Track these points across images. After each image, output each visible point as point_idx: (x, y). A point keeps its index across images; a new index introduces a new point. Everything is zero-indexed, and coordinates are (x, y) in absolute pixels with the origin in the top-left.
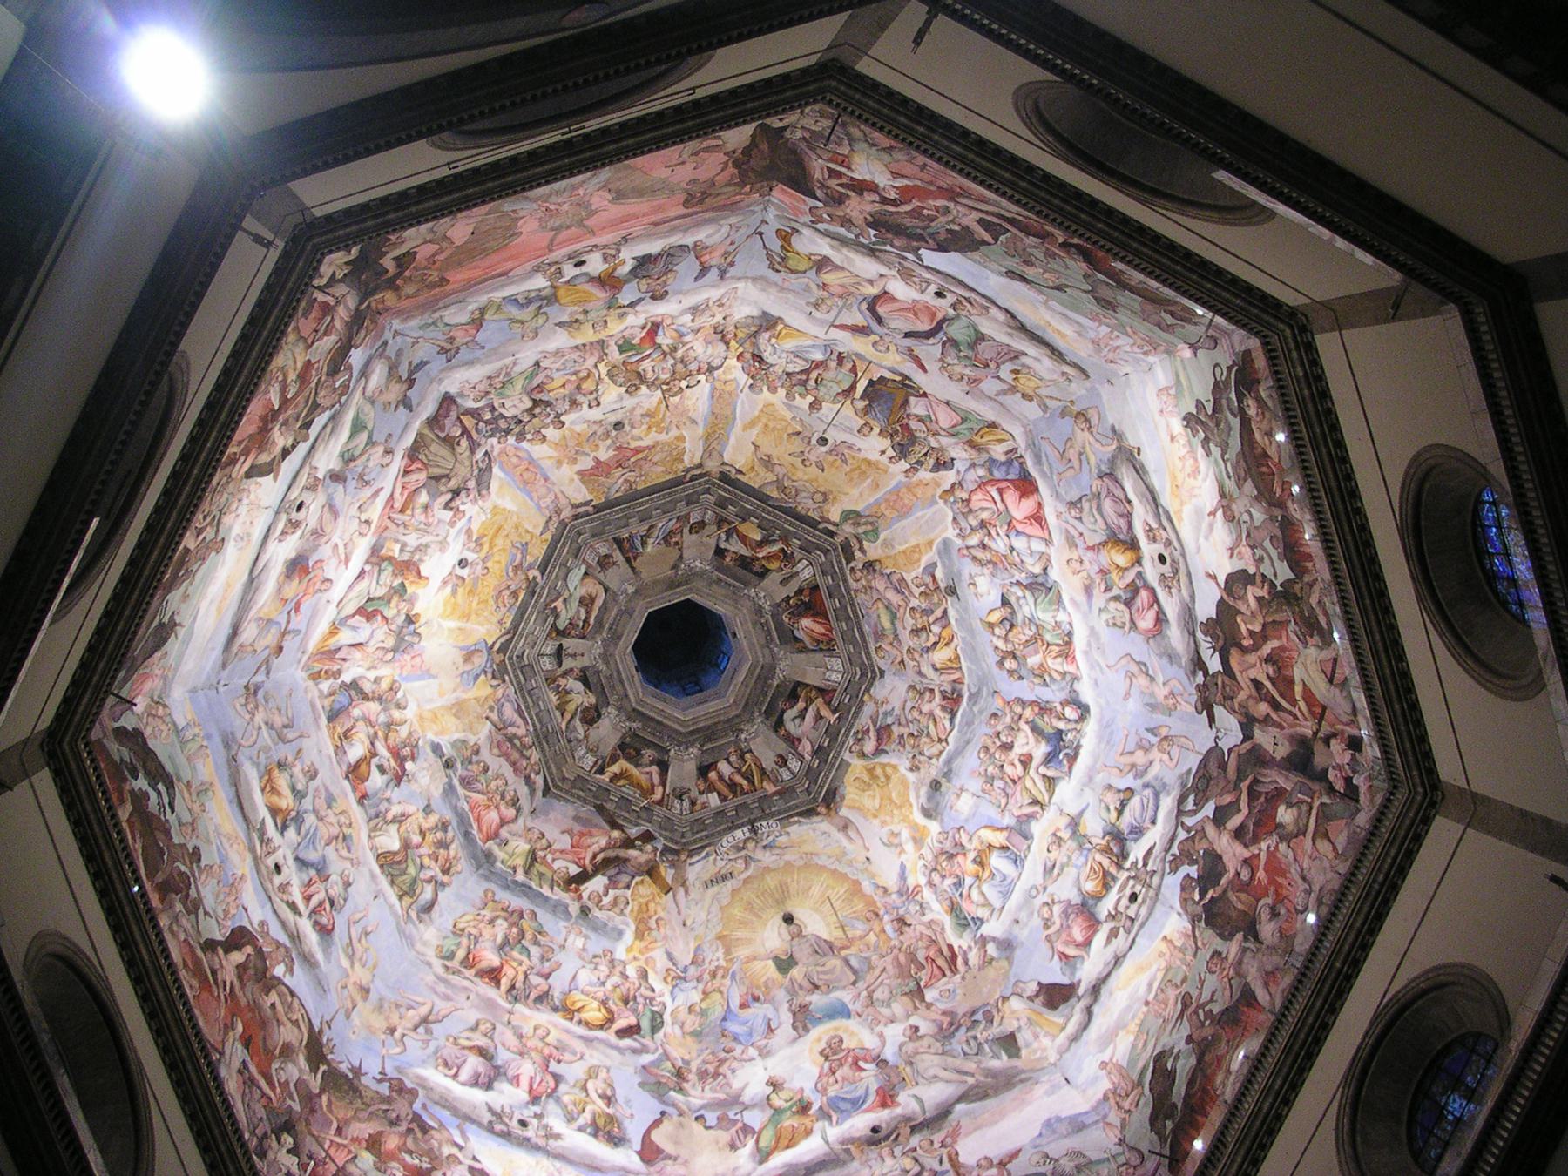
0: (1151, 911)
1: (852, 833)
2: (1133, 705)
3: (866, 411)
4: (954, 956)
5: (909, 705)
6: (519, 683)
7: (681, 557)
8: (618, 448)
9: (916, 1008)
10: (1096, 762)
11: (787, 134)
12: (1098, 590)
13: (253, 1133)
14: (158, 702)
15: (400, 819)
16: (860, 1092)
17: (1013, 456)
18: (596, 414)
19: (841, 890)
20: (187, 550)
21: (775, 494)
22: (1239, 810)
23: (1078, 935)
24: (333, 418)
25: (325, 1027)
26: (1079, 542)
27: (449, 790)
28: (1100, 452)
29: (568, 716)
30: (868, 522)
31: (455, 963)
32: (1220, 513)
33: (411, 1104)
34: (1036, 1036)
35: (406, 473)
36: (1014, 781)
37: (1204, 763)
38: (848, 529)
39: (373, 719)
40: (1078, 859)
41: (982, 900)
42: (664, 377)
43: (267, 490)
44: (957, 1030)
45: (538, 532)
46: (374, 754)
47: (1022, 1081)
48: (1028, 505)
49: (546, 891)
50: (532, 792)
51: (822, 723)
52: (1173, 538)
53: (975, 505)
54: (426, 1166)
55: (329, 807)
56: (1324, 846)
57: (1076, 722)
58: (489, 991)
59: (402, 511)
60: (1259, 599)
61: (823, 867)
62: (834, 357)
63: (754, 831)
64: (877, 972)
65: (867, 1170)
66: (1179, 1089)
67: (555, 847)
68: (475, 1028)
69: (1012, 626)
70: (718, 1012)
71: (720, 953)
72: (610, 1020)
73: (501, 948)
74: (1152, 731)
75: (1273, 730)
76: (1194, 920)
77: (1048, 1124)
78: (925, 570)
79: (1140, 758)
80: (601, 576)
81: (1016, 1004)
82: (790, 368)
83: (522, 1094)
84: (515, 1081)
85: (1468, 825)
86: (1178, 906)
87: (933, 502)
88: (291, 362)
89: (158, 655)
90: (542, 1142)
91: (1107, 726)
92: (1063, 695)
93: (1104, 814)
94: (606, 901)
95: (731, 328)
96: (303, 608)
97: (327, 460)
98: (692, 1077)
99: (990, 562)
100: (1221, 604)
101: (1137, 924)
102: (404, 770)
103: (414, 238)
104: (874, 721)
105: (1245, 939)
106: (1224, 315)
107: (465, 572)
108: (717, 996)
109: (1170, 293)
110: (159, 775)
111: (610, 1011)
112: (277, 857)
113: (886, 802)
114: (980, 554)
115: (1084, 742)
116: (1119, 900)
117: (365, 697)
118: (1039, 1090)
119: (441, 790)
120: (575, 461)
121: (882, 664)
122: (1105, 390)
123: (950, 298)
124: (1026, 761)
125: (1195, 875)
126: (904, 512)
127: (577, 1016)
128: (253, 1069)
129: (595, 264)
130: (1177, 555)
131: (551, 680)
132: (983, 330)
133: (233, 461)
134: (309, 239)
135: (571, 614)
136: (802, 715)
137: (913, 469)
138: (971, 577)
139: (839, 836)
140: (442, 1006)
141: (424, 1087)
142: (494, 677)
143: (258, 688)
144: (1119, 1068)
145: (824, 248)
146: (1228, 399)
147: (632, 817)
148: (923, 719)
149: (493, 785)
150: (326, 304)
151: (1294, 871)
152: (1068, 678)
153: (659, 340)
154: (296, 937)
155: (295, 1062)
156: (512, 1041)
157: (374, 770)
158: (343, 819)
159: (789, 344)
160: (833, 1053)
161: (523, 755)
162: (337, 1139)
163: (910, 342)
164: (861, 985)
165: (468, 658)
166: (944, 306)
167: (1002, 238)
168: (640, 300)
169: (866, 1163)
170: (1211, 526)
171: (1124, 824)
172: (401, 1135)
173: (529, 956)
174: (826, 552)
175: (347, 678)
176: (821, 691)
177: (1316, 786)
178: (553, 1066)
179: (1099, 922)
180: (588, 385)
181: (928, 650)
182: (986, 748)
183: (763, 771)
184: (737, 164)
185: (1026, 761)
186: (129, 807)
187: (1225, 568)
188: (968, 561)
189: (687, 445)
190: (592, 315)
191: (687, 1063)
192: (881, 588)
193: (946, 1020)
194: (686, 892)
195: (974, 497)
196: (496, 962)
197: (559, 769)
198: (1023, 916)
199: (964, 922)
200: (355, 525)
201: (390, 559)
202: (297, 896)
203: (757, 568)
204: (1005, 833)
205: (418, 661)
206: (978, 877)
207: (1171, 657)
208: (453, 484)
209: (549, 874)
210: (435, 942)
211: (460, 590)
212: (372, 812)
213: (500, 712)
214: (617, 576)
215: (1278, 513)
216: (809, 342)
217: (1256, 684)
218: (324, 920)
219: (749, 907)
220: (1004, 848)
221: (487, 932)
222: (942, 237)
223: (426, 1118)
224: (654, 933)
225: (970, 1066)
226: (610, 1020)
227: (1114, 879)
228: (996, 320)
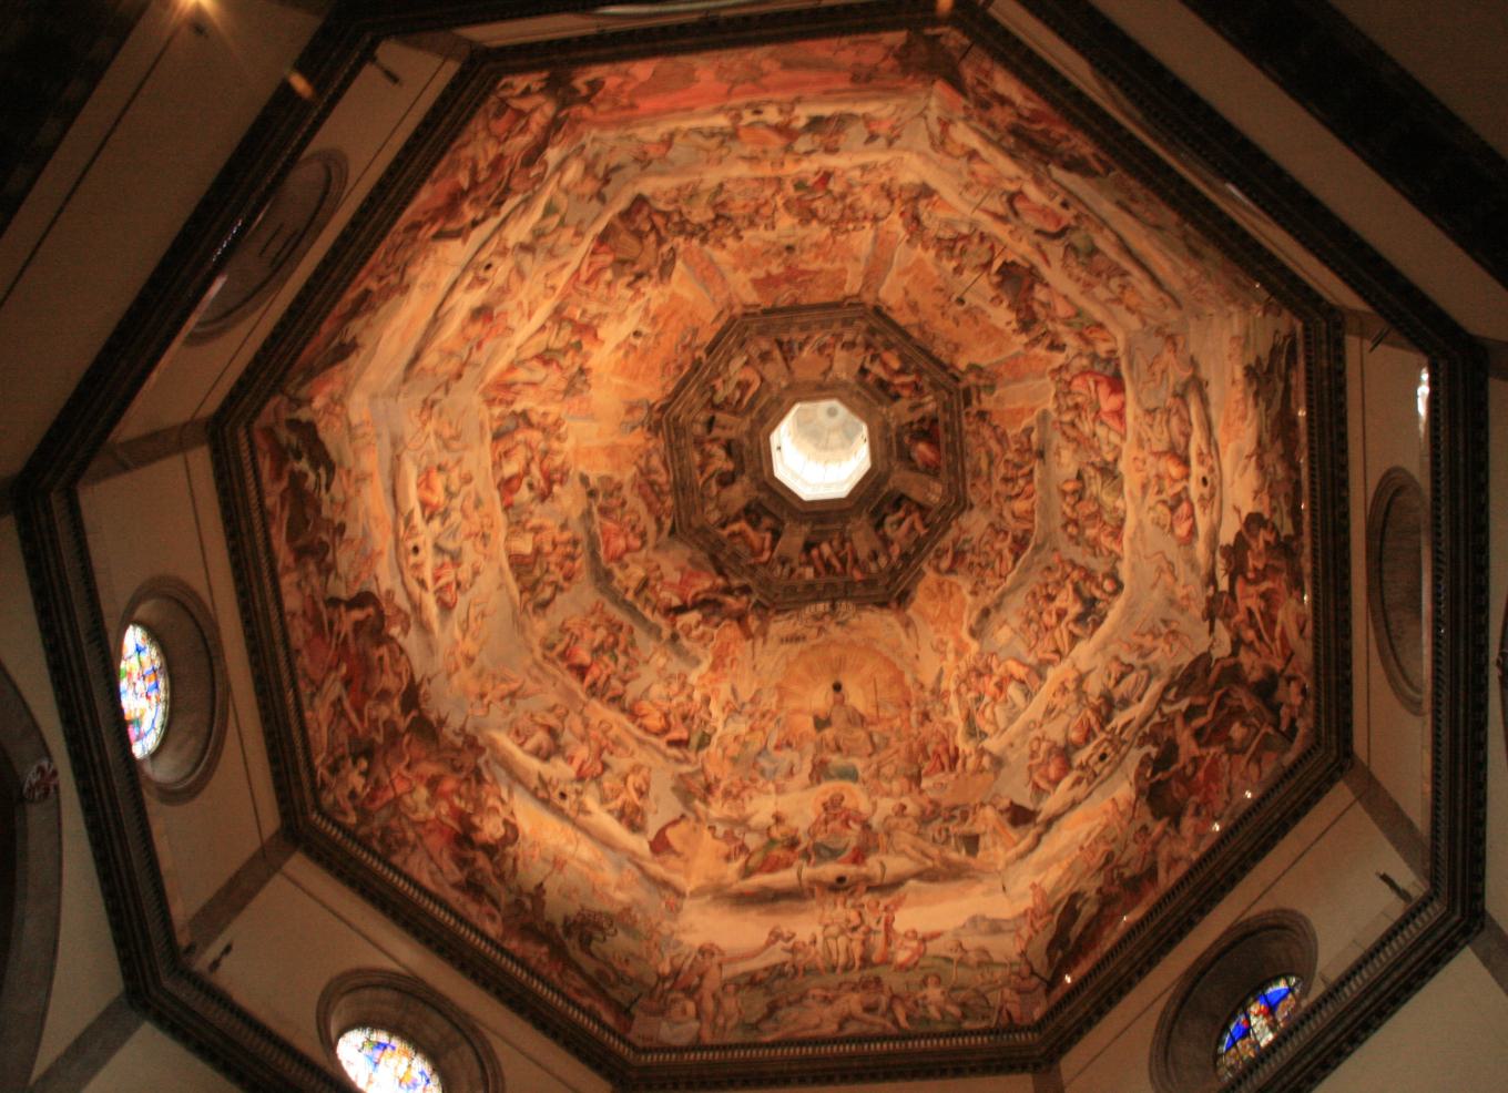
0: (1111, 773)
1: (911, 631)
2: (1156, 594)
3: (999, 285)
5: (985, 539)
6: (670, 440)
7: (830, 368)
8: (789, 267)
9: (910, 790)
11: (943, 40)
12: (1153, 490)
13: (330, 753)
14: (338, 401)
15: (537, 530)
16: (841, 845)
17: (1111, 358)
18: (771, 235)
19: (887, 675)
20: (367, 292)
21: (916, 334)
22: (1206, 713)
23: (1053, 771)
25: (425, 682)
26: (1147, 445)
27: (587, 515)
28: (1178, 374)
29: (706, 475)
30: (988, 379)
31: (554, 654)
32: (1254, 458)
33: (476, 759)
34: (995, 844)
35: (594, 253)
36: (1047, 629)
37: (1194, 664)
38: (971, 379)
39: (534, 445)
40: (1073, 710)
43: (456, 253)
44: (936, 818)
45: (711, 320)
47: (970, 877)
49: (647, 613)
50: (660, 529)
56: (1253, 769)
58: (575, 684)
59: (588, 282)
60: (1267, 543)
61: (878, 653)
62: (977, 233)
63: (833, 607)
65: (818, 911)
66: (1077, 929)
67: (667, 579)
68: (552, 709)
69: (1080, 499)
70: (756, 746)
71: (774, 700)
72: (666, 730)
74: (1165, 622)
75: (1254, 656)
76: (1140, 792)
77: (974, 920)
78: (1024, 431)
79: (1148, 641)
80: (760, 368)
81: (989, 812)
82: (941, 234)
83: (571, 771)
84: (570, 760)
85: (1359, 798)
86: (1132, 776)
87: (1042, 376)
89: (338, 367)
90: (572, 814)
91: (1131, 607)
93: (1105, 679)
94: (695, 633)
95: (895, 189)
96: (487, 346)
97: (518, 232)
98: (718, 793)
99: (1075, 439)
100: (1239, 535)
101: (1098, 780)
102: (550, 491)
103: (596, 72)
104: (954, 544)
105: (1169, 824)
107: (638, 342)
108: (760, 734)
110: (323, 460)
111: (668, 723)
112: (419, 541)
114: (1072, 433)
116: (1091, 756)
117: (530, 425)
118: (979, 889)
119: (579, 512)
120: (748, 269)
121: (973, 497)
122: (1193, 322)
124: (1061, 614)
125: (1154, 755)
126: (1018, 378)
127: (639, 721)
129: (772, 115)
130: (1216, 482)
133: (417, 226)
135: (726, 393)
136: (900, 522)
137: (1035, 342)
139: (899, 629)
140: (530, 685)
144: (1043, 892)
145: (974, 142)
146: (1280, 365)
148: (993, 555)
149: (627, 518)
151: (1224, 783)
153: (831, 185)
154: (418, 607)
155: (388, 704)
156: (578, 726)
158: (486, 521)
159: (942, 214)
160: (833, 807)
161: (658, 499)
162: (405, 773)
163: (1037, 238)
166: (1068, 216)
167: (1112, 174)
169: (822, 905)
170: (1245, 468)
171: (1118, 693)
173: (616, 661)
174: (950, 394)
175: (518, 407)
177: (1269, 716)
178: (606, 756)
180: (765, 211)
181: (1011, 498)
182: (1034, 594)
183: (856, 561)
184: (895, 56)
185: (1061, 614)
186: (284, 483)
187: (1248, 507)
189: (849, 277)
190: (771, 155)
193: (930, 808)
194: (765, 642)
198: (1018, 742)
199: (973, 732)
200: (541, 288)
201: (571, 321)
202: (428, 575)
203: (892, 390)
204: (1026, 670)
205: (585, 405)
206: (994, 699)
207: (1193, 565)
208: (637, 268)
209: (654, 600)
212: (514, 519)
213: (648, 461)
214: (774, 371)
215: (1294, 476)
216: (958, 217)
217: (1250, 612)
218: (448, 598)
219: (810, 669)
220: (1022, 682)
221: (588, 634)
222: (1066, 158)
224: (726, 670)
225: (934, 851)
226: (666, 730)
227: (1095, 736)
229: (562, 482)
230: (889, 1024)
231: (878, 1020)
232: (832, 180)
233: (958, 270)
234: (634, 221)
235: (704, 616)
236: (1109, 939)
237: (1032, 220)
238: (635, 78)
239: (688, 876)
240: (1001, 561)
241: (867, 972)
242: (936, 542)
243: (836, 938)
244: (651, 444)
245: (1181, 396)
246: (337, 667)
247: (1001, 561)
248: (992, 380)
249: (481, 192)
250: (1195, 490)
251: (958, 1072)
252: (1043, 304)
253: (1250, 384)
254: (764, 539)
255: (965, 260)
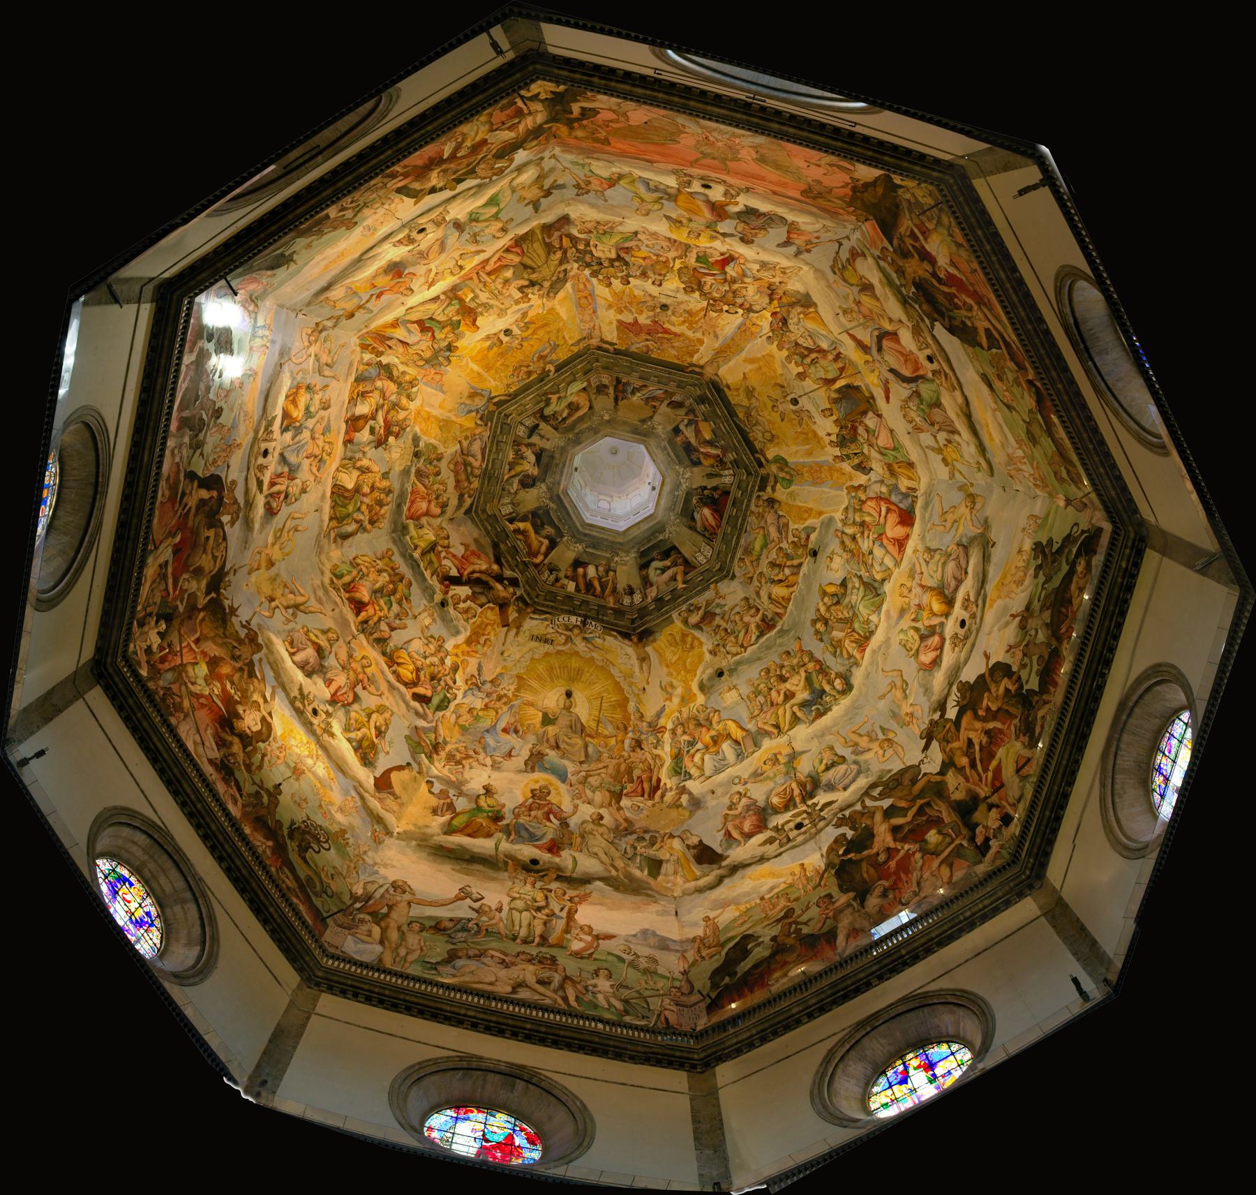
1: (645, 667)
3: (836, 401)
4: (657, 787)
5: (737, 609)
6: (495, 432)
7: (651, 417)
8: (655, 322)
9: (610, 804)
10: (834, 725)
12: (908, 617)
15: (364, 471)
16: (539, 833)
18: (654, 290)
21: (741, 415)
23: (747, 826)
24: (479, 186)
26: (917, 577)
27: (406, 472)
28: (968, 528)
29: (513, 473)
30: (790, 473)
31: (339, 583)
32: (1018, 619)
33: (253, 653)
34: (675, 873)
35: (508, 250)
36: (772, 704)
38: (774, 469)
40: (780, 779)
41: (699, 763)
42: (715, 295)
45: (571, 342)
46: (374, 418)
47: (647, 895)
48: (900, 531)
49: (427, 574)
51: (673, 583)
52: (979, 614)
53: (866, 508)
54: (236, 697)
55: (323, 434)
57: (838, 692)
58: (350, 616)
59: (489, 274)
62: (835, 353)
63: (584, 623)
64: (600, 765)
68: (325, 632)
69: (838, 603)
70: (487, 723)
71: (512, 688)
72: (414, 684)
73: (375, 592)
77: (645, 932)
80: (593, 397)
81: (676, 844)
82: (801, 341)
83: (327, 694)
84: (328, 682)
88: (473, 134)
90: (319, 731)
92: (841, 669)
93: (816, 764)
94: (462, 605)
95: (780, 292)
98: (443, 754)
99: (851, 551)
103: (603, 102)
104: (708, 603)
106: (1099, 495)
107: (505, 339)
109: (1075, 458)
111: (418, 677)
112: (270, 446)
113: (681, 662)
115: (835, 708)
117: (391, 378)
118: (654, 908)
120: (621, 312)
121: (738, 571)
123: (935, 366)
124: (789, 696)
126: (817, 482)
127: (395, 667)
128: (170, 570)
129: (717, 194)
130: (974, 627)
131: (517, 443)
132: (943, 401)
134: (534, 63)
135: (557, 409)
136: (663, 570)
138: (833, 553)
139: (635, 662)
140: (313, 603)
141: (268, 648)
142: (481, 419)
143: (324, 329)
145: (875, 278)
146: (1070, 551)
147: (513, 563)
148: (740, 623)
150: (521, 109)
152: (852, 660)
153: (728, 269)
154: (249, 504)
155: (198, 582)
156: (343, 655)
157: (367, 428)
158: (327, 447)
159: (810, 325)
160: (539, 796)
161: (468, 479)
163: (890, 376)
164: (585, 766)
165: (472, 395)
166: (928, 368)
168: (732, 235)
170: (1007, 624)
172: (234, 668)
173: (389, 609)
174: (749, 474)
176: (686, 562)
179: (766, 827)
181: (773, 582)
182: (768, 671)
183: (614, 590)
186: (193, 357)
188: (837, 542)
189: (702, 349)
190: (691, 225)
191: (445, 742)
192: (769, 521)
193: (624, 825)
194: (517, 634)
195: (869, 503)
196: (366, 599)
197: (485, 503)
198: (719, 791)
199: (678, 770)
200: (451, 264)
201: (461, 301)
205: (438, 377)
206: (707, 747)
208: (534, 277)
209: (436, 565)
210: (335, 561)
211: (495, 349)
212: (349, 454)
213: (470, 444)
214: (604, 403)
216: (824, 332)
218: (274, 505)
219: (550, 669)
220: (737, 742)
221: (373, 576)
223: (257, 668)
224: (479, 647)
225: (620, 864)
226: (414, 684)
228: (955, 400)
229: (397, 436)
230: (560, 1001)
231: (548, 993)
232: (732, 265)
233: (801, 376)
234: (549, 237)
235: (474, 593)
236: (778, 983)
237: (892, 360)
238: (628, 119)
239: (398, 819)
240: (746, 632)
241: (544, 950)
242: (691, 598)
243: (521, 912)
244: (478, 431)
245: (965, 548)
246: (174, 536)
247: (746, 632)
248: (791, 476)
249: (452, 165)
250: (951, 627)
251: (619, 1056)
252: (867, 430)
253: (1035, 558)
254: (542, 543)
255: (812, 369)
